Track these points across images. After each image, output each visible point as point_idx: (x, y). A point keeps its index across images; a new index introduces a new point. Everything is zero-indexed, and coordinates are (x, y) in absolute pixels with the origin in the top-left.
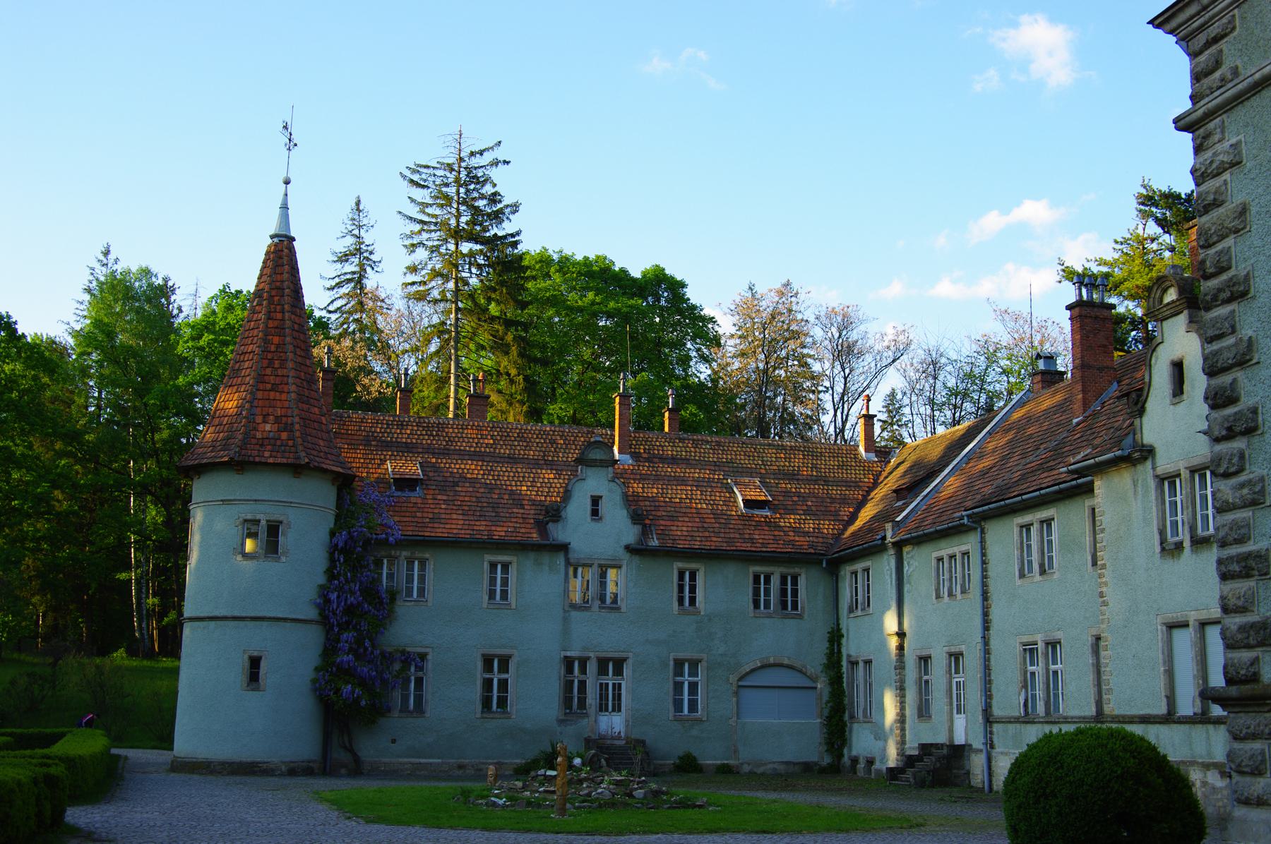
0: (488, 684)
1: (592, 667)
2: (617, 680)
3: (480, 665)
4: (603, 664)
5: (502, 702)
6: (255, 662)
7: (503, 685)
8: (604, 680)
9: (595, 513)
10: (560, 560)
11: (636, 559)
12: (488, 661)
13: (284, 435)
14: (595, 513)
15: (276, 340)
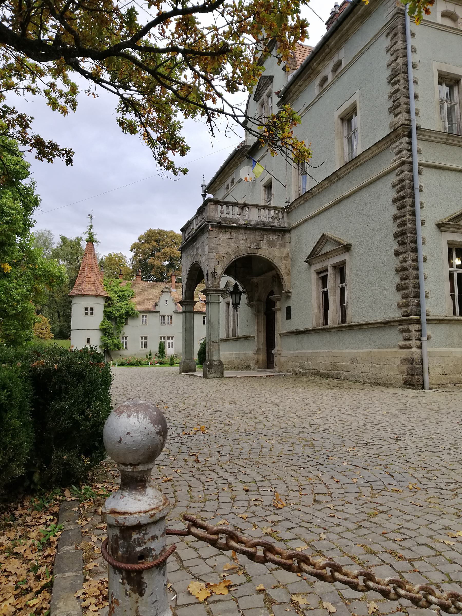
0: (142, 343)
1: (166, 338)
2: (172, 341)
3: (140, 338)
4: (169, 338)
5: (145, 347)
6: (88, 339)
7: (146, 343)
8: (169, 341)
9: (166, 303)
10: (158, 314)
11: (176, 314)
12: (142, 338)
13: (93, 288)
14: (166, 303)
15: (90, 265)
